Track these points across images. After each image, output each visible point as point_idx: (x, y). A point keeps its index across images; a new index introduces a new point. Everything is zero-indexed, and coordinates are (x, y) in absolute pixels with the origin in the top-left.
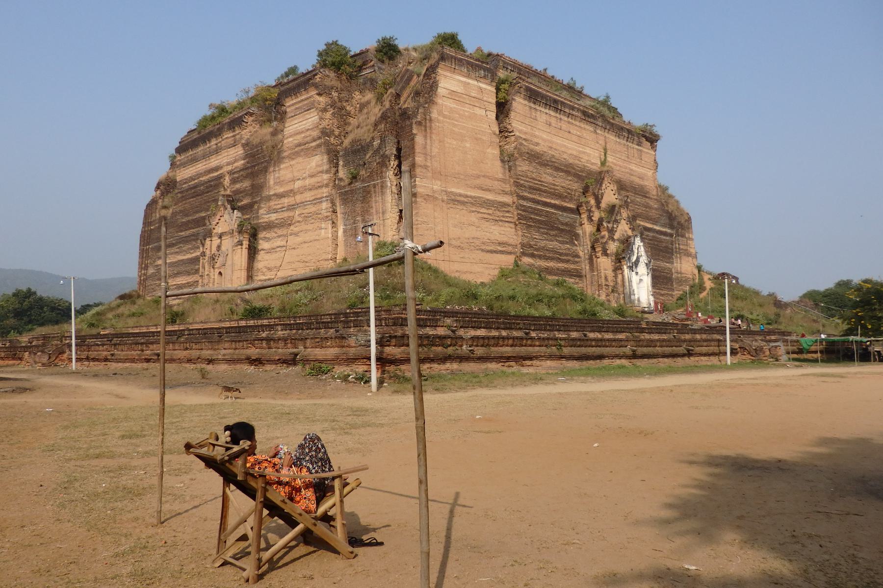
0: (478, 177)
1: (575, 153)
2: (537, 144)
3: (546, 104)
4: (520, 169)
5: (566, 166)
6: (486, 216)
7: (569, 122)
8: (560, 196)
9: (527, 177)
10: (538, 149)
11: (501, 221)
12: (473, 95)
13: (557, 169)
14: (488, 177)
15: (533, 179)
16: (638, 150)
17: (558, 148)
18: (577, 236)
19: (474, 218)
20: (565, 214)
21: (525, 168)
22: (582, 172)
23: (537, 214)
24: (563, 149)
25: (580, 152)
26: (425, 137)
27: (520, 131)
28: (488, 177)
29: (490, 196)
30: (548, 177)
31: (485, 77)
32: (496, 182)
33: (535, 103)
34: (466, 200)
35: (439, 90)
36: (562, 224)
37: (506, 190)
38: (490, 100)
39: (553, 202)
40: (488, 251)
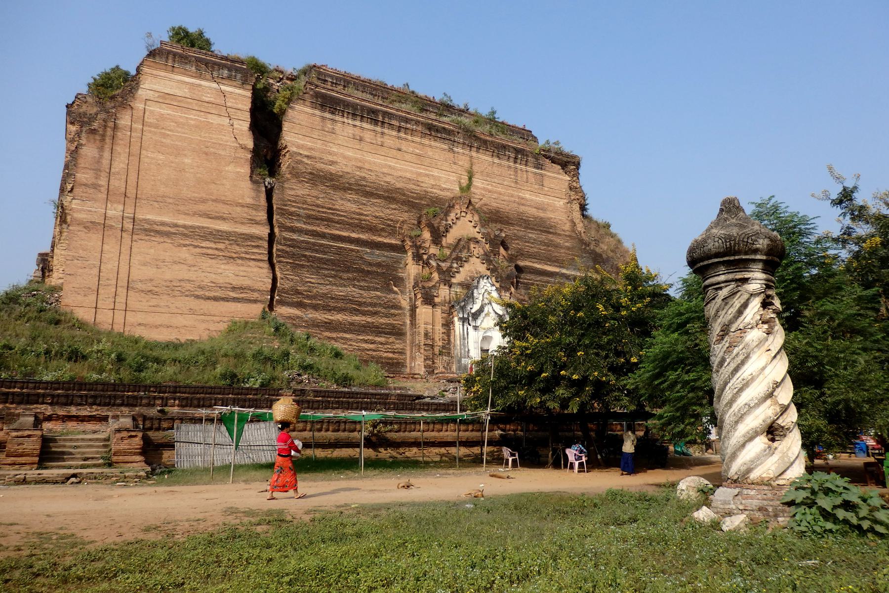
0: (204, 201)
1: (408, 175)
2: (332, 163)
3: (354, 115)
4: (292, 193)
5: (387, 191)
6: (210, 251)
7: (399, 138)
8: (372, 229)
11: (242, 258)
12: (207, 99)
13: (369, 194)
14: (224, 203)
15: (318, 206)
16: (535, 173)
17: (374, 168)
18: (399, 281)
19: (184, 254)
20: (377, 252)
21: (300, 192)
22: (421, 199)
23: (317, 251)
24: (385, 170)
25: (419, 174)
26: (101, 149)
27: (298, 147)
28: (224, 203)
29: (224, 227)
30: (347, 204)
31: (229, 78)
32: (239, 209)
33: (333, 113)
34: (173, 230)
35: (140, 92)
36: (370, 264)
37: (258, 219)
38: (240, 106)
39: (354, 235)
40: (209, 298)
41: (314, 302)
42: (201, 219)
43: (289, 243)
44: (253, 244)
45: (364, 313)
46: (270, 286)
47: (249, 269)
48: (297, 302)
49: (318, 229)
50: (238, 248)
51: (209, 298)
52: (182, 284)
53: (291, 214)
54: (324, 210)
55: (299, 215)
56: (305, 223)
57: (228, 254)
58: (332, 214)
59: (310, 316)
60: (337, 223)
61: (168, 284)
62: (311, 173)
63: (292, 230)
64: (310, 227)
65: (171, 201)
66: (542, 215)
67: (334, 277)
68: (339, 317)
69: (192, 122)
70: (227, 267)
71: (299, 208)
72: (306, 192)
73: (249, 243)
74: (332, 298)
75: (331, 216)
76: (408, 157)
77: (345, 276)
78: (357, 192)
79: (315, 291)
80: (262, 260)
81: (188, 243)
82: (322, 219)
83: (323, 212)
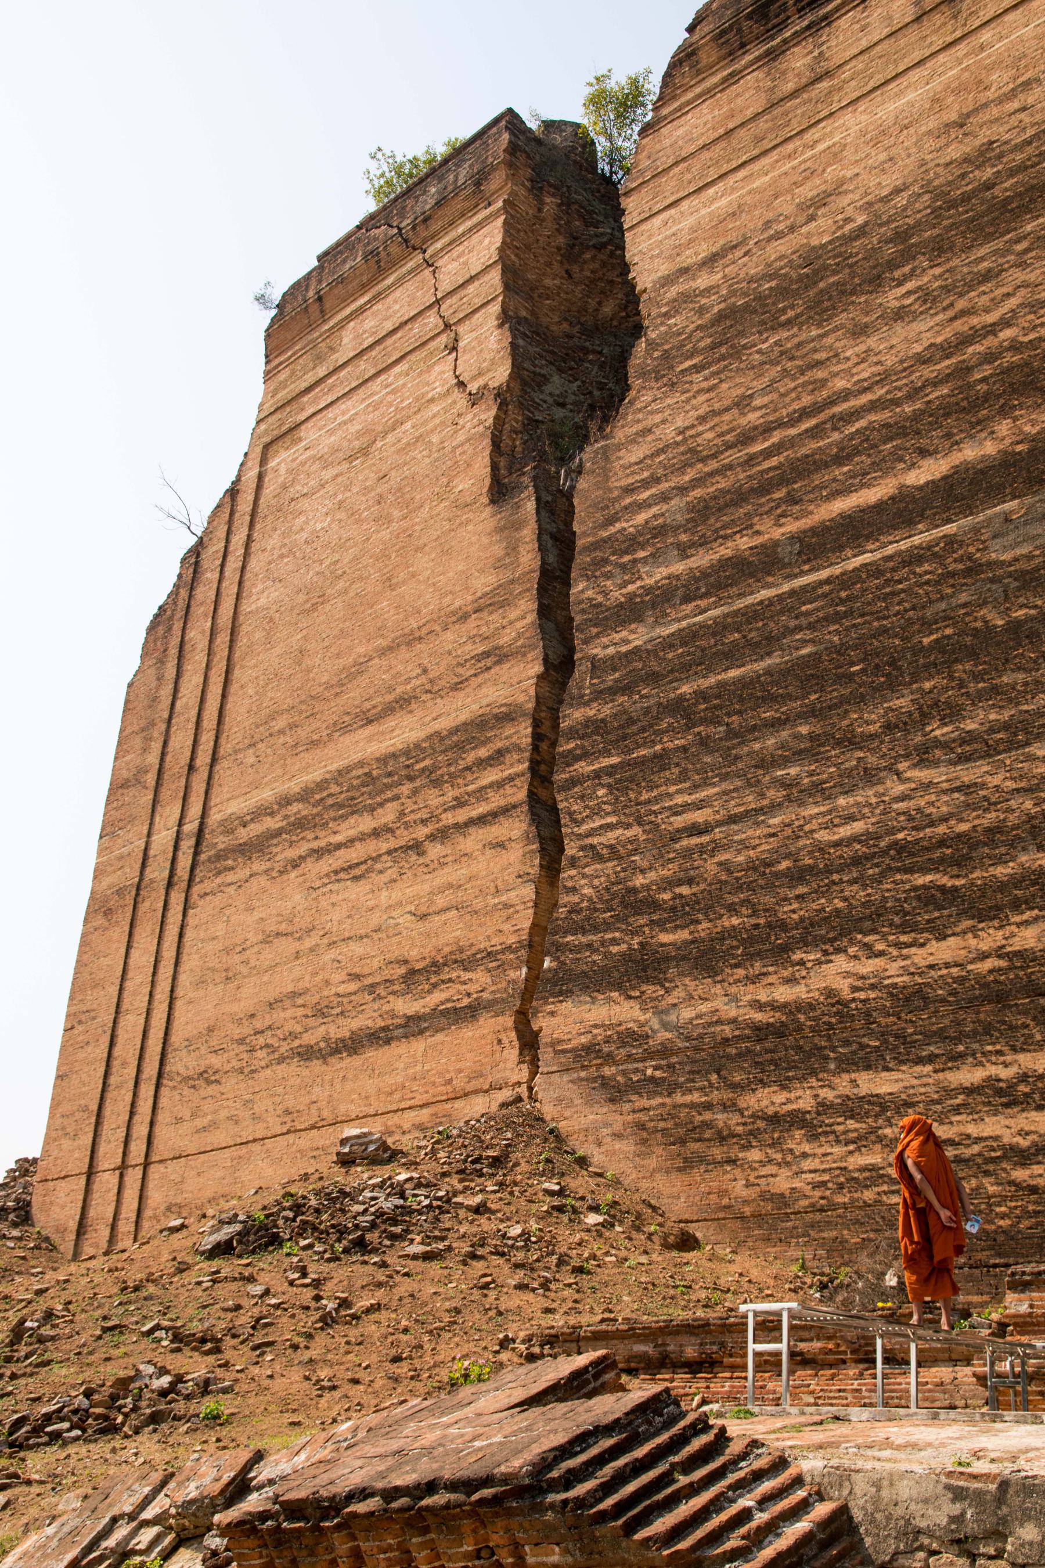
6: (353, 854)
9: (695, 456)
10: (821, 231)
11: (442, 835)
14: (412, 640)
15: (746, 438)
19: (291, 897)
23: (731, 656)
29: (405, 731)
37: (506, 638)
41: (704, 927)
42: (348, 740)
43: (611, 678)
44: (483, 752)
45: (987, 907)
46: (525, 920)
47: (460, 873)
48: (627, 957)
49: (744, 542)
50: (433, 798)
51: (352, 1045)
52: (279, 1015)
53: (632, 543)
54: (776, 437)
55: (661, 531)
56: (684, 551)
57: (404, 837)
58: (814, 433)
59: (687, 1014)
60: (839, 460)
61: (247, 1030)
62: (721, 317)
63: (630, 612)
64: (702, 560)
65: (280, 723)
67: (810, 751)
68: (838, 973)
69: (354, 428)
70: (396, 895)
71: (664, 498)
72: (701, 404)
73: (471, 757)
74: (798, 875)
75: (812, 445)
77: (870, 719)
78: (940, 249)
79: (710, 867)
80: (505, 811)
81: (303, 848)
82: (764, 488)
83: (767, 454)
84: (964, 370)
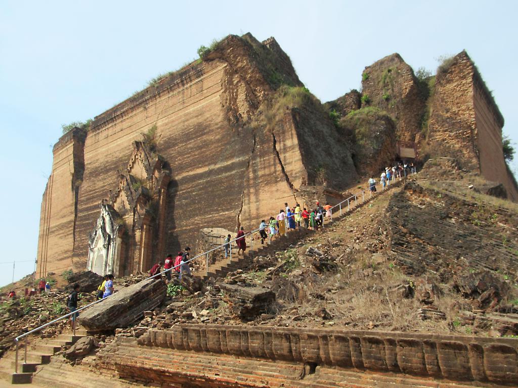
10: (97, 165)
62: (90, 173)
66: (200, 119)
76: (125, 132)
84: (103, 190)
